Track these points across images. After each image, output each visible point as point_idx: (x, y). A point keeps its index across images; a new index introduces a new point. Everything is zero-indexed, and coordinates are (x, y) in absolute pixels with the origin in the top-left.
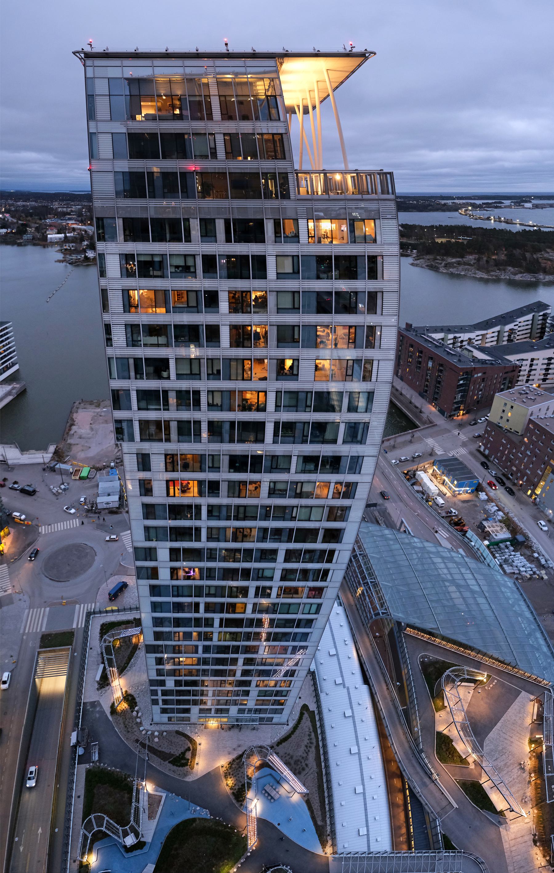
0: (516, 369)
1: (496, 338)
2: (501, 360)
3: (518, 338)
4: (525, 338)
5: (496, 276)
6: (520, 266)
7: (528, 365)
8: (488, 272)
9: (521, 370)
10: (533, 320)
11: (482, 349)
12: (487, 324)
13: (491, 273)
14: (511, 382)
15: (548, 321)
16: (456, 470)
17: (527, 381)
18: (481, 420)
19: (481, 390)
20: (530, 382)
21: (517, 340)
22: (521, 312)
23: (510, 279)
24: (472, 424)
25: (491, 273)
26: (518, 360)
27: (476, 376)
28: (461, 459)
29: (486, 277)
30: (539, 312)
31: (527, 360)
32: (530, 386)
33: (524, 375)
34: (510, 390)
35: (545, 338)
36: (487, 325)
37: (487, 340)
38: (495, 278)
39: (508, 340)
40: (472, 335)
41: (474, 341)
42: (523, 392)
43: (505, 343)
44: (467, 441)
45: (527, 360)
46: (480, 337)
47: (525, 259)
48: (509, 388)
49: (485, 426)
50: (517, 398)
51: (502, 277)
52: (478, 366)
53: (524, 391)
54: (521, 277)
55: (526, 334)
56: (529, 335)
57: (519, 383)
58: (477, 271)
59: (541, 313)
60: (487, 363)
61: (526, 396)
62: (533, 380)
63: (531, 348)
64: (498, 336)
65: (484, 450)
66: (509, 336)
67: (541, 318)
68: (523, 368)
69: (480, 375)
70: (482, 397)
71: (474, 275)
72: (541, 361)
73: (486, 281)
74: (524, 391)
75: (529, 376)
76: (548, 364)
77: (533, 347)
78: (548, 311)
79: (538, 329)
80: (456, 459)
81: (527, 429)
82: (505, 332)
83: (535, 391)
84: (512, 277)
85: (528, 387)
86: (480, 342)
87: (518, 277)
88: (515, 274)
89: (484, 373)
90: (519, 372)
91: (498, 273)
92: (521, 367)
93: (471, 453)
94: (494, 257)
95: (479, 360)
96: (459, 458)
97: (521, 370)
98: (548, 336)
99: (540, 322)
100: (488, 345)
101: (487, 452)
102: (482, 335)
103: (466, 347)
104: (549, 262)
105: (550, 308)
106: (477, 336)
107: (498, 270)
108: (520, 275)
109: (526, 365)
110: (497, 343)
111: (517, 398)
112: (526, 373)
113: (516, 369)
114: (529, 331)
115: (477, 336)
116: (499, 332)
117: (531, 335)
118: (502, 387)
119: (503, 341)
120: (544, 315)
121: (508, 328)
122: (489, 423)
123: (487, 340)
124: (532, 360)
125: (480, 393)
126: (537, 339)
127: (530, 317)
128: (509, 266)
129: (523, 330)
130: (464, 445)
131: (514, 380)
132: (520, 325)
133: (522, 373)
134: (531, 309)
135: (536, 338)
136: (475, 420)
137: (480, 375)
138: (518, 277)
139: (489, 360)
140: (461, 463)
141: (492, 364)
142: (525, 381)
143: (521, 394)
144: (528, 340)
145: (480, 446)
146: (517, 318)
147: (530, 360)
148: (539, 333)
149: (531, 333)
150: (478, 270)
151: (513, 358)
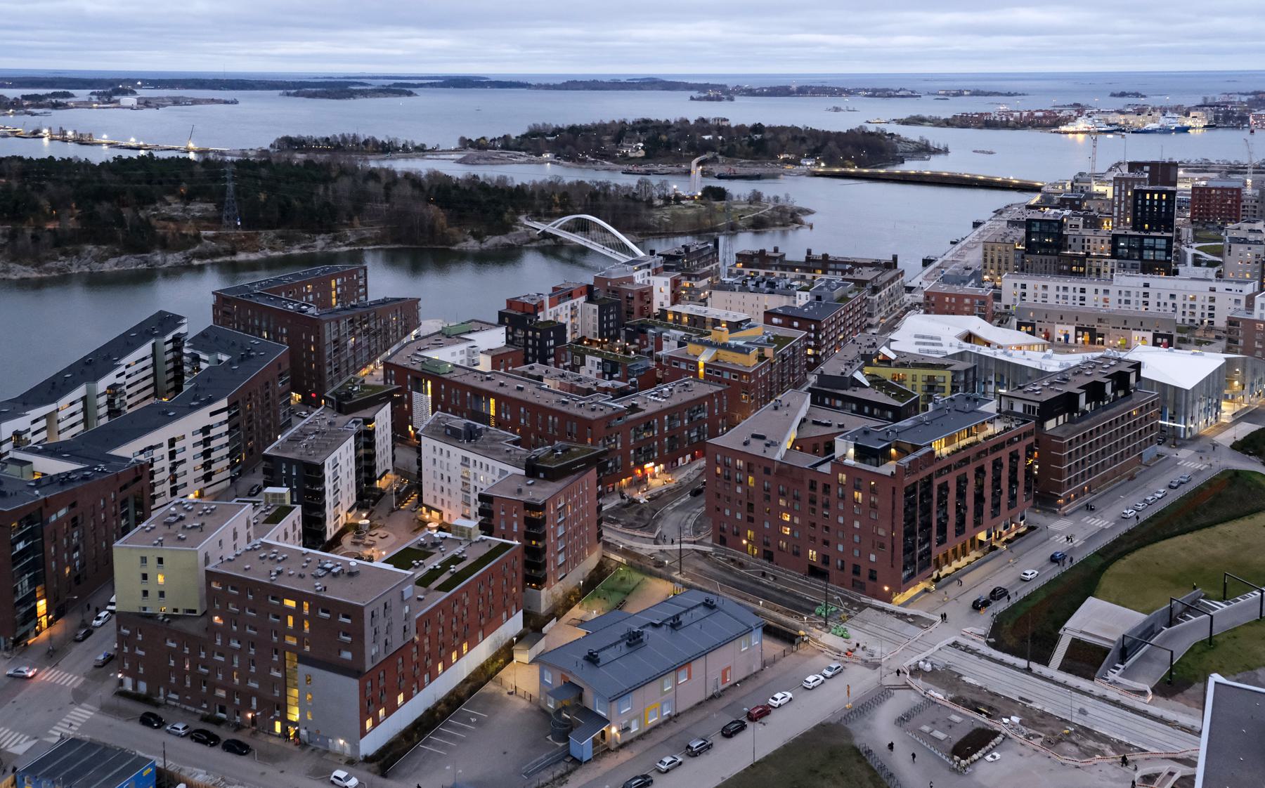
0: (143, 472)
1: (80, 416)
2: (103, 462)
3: (129, 402)
4: (146, 398)
5: (59, 270)
6: (111, 240)
7: (167, 456)
8: (38, 263)
9: (153, 473)
10: (154, 355)
11: (52, 451)
12: (53, 388)
13: (47, 265)
14: (139, 506)
15: (186, 351)
16: (86, 767)
17: (174, 492)
18: (98, 619)
19: (77, 548)
20: (180, 492)
21: (130, 407)
22: (126, 343)
23: (91, 273)
24: (80, 637)
25: (47, 265)
26: (142, 452)
27: (53, 518)
28: (87, 737)
29: (33, 274)
30: (164, 334)
31: (161, 445)
32: (184, 501)
33: (163, 481)
34: (144, 525)
35: (186, 388)
36: (53, 389)
37: (62, 426)
38: (54, 274)
39: (109, 413)
40: (21, 423)
41: (29, 435)
42: (173, 519)
43: (104, 421)
44: (85, 683)
45: (161, 445)
46: (43, 423)
47: (121, 222)
48: (139, 520)
49: (115, 627)
50: (165, 535)
51: (74, 270)
52: (54, 492)
53: (175, 515)
54: (116, 265)
55: (145, 389)
56: (151, 390)
57: (159, 502)
58: (11, 265)
59: (169, 337)
60: (72, 481)
61: (181, 524)
62: (185, 485)
63: (162, 417)
64: (85, 409)
65: (135, 686)
66: (110, 402)
67: (169, 346)
68: (156, 466)
69: (62, 513)
70: (83, 565)
71: (5, 276)
72: (191, 439)
73: (38, 285)
74: (175, 515)
75: (174, 481)
76: (206, 442)
77: (165, 413)
78: (182, 330)
79: (167, 372)
80: (74, 742)
81: (211, 596)
82: (98, 396)
83: (196, 507)
84: (97, 267)
85: (180, 503)
86: (43, 435)
87: (109, 266)
88: (103, 259)
89: (73, 505)
90: (152, 478)
91: (62, 262)
92: (151, 465)
93: (106, 709)
94: (50, 226)
95: (52, 478)
96: (79, 735)
97: (153, 473)
98: (190, 382)
99: (170, 356)
100: (65, 437)
101: (143, 687)
102: (45, 416)
103: (11, 455)
104: (172, 225)
105: (185, 321)
106: (34, 422)
107: (62, 254)
108: (113, 261)
109: (163, 457)
110: (86, 426)
111: (165, 535)
112: (167, 473)
113: (143, 472)
114: (150, 381)
115: (34, 422)
116: (84, 399)
117: (156, 389)
118: (123, 522)
119: (99, 418)
120: (176, 339)
121: (103, 385)
122: (122, 618)
123: (62, 426)
124: (172, 442)
125: (76, 555)
126: (171, 394)
127: (146, 349)
128: (87, 241)
129: (137, 382)
130: (79, 697)
131: (146, 501)
132: (128, 371)
133: (157, 478)
134: (147, 332)
135: (168, 392)
136: (84, 624)
137: (62, 513)
138: (109, 266)
139: (75, 472)
140: (92, 745)
141: (85, 478)
142: (168, 493)
143: (169, 524)
144: (152, 401)
145: (121, 682)
146: (122, 356)
147: (166, 444)
148: (171, 380)
149: (155, 384)
150: (13, 260)
151: (129, 451)
